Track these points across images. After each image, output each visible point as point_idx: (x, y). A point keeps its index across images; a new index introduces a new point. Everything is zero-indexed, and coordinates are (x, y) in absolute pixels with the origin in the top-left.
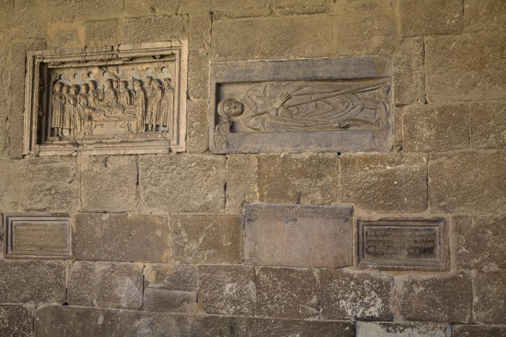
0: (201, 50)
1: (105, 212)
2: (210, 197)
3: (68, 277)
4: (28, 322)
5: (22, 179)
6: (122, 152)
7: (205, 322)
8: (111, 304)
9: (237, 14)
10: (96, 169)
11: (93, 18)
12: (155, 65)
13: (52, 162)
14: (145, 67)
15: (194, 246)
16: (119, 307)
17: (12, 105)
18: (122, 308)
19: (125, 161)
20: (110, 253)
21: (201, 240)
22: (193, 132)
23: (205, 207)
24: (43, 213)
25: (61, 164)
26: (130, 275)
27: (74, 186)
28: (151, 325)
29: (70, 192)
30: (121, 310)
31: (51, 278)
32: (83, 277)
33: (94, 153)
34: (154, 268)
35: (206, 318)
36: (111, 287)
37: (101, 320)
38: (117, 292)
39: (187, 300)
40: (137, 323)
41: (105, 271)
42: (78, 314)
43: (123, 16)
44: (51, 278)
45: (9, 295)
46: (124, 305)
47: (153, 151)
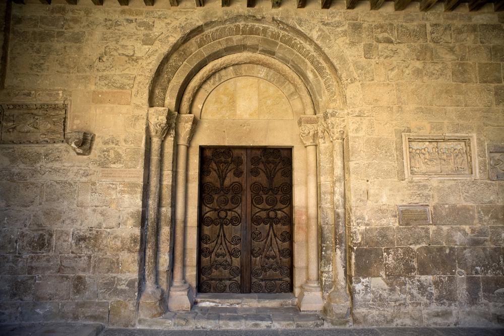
0: (482, 138)
1: (447, 204)
2: (492, 198)
3: (431, 233)
4: (413, 254)
5: (405, 190)
6: (452, 179)
7: (495, 250)
8: (452, 244)
9: (496, 124)
10: (441, 185)
11: (432, 121)
12: (456, 143)
13: (420, 182)
14: (451, 143)
15: (487, 218)
16: (457, 245)
17: (397, 156)
18: (457, 245)
19: (453, 183)
20: (450, 222)
21: (490, 215)
22: (481, 172)
23: (491, 202)
24: (417, 205)
25: (424, 183)
26: (460, 231)
27: (431, 193)
28: (471, 252)
29: (429, 196)
30: (456, 246)
31: (423, 234)
32: (438, 232)
33: (439, 178)
34: (470, 228)
35: (495, 248)
36: (452, 236)
37: (447, 251)
38: (454, 238)
39: (486, 240)
40: (465, 252)
41: (448, 230)
42: (437, 249)
43: (446, 122)
44: (423, 234)
45: (402, 242)
46: (458, 244)
47: (465, 179)
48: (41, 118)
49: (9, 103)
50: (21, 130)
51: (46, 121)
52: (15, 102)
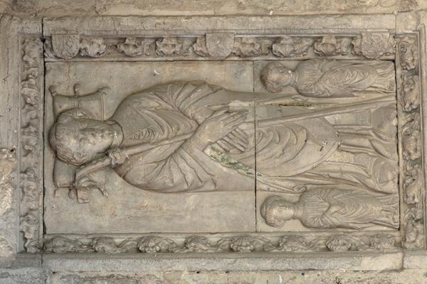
48: (261, 112)
49: (87, 27)
50: (160, 180)
51: (295, 129)
52: (126, 22)
